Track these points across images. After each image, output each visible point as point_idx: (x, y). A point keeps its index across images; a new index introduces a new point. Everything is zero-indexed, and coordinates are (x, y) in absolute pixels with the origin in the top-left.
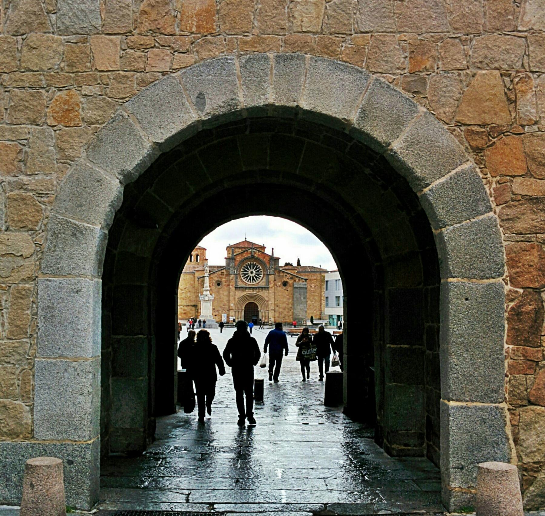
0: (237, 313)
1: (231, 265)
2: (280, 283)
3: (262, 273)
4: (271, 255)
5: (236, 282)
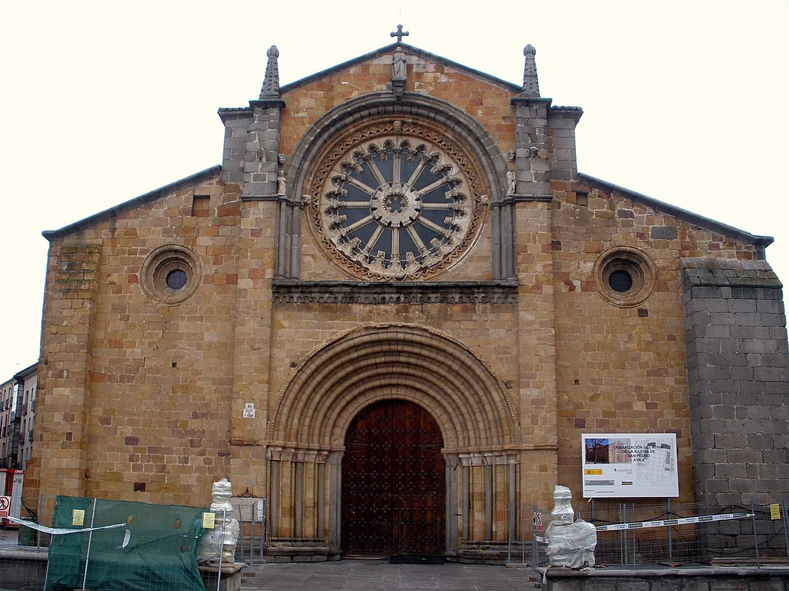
0: (287, 471)
2: (588, 267)
3: (467, 206)
4: (519, 82)
5: (282, 255)
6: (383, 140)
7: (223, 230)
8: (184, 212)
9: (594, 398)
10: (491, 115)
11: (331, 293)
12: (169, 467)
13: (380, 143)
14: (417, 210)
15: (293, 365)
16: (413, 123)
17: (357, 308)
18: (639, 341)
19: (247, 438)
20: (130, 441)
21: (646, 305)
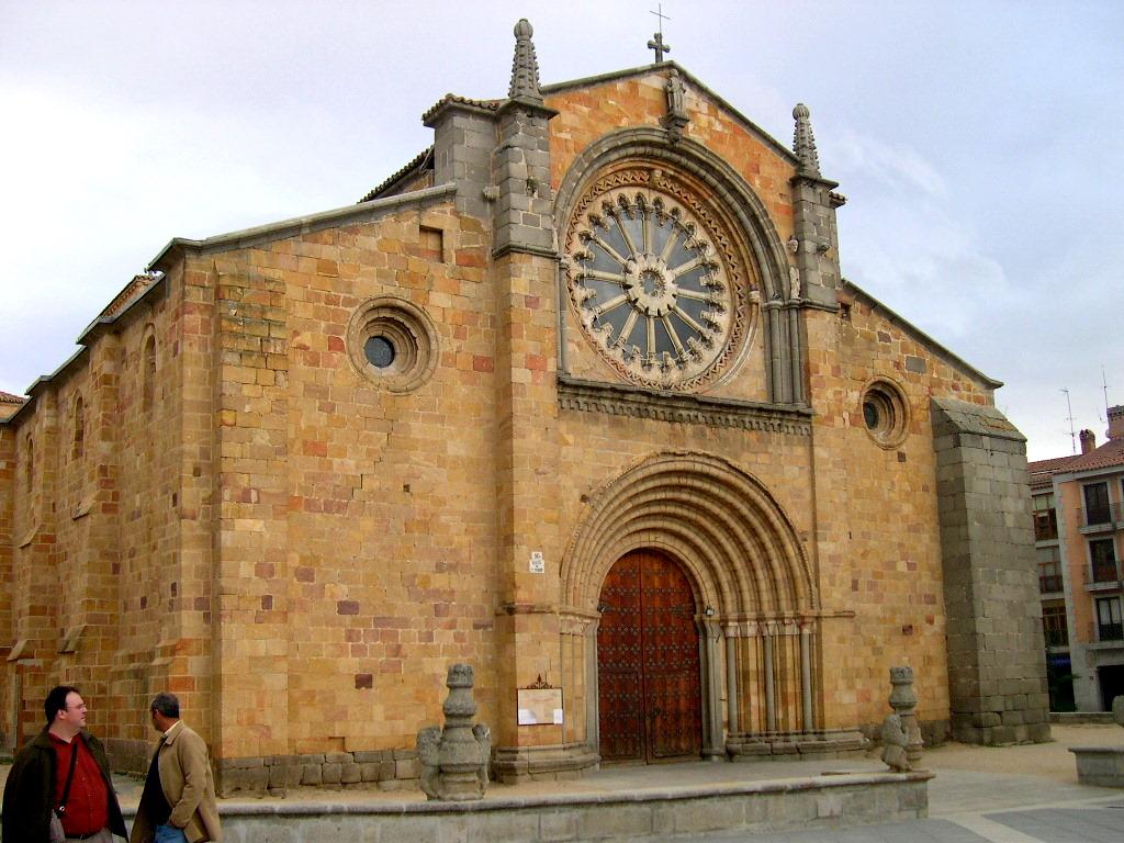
1: (518, 169)
3: (724, 299)
6: (635, 191)
7: (467, 288)
8: (411, 250)
9: (864, 555)
10: (768, 185)
11: (622, 401)
12: (406, 649)
13: (630, 194)
14: (674, 296)
15: (584, 498)
16: (672, 177)
17: (649, 423)
18: (900, 490)
19: (536, 601)
20: (346, 608)
21: (904, 449)
